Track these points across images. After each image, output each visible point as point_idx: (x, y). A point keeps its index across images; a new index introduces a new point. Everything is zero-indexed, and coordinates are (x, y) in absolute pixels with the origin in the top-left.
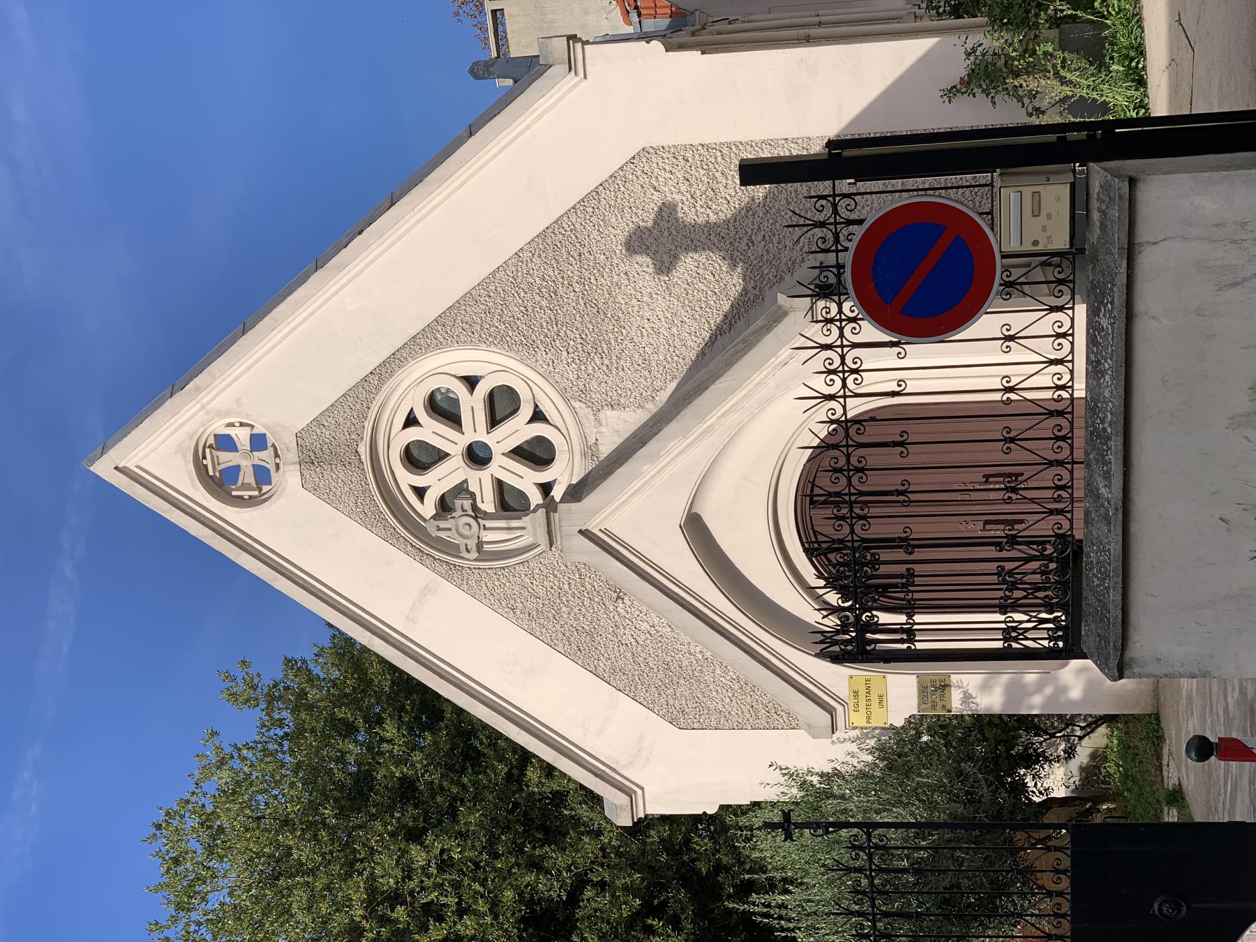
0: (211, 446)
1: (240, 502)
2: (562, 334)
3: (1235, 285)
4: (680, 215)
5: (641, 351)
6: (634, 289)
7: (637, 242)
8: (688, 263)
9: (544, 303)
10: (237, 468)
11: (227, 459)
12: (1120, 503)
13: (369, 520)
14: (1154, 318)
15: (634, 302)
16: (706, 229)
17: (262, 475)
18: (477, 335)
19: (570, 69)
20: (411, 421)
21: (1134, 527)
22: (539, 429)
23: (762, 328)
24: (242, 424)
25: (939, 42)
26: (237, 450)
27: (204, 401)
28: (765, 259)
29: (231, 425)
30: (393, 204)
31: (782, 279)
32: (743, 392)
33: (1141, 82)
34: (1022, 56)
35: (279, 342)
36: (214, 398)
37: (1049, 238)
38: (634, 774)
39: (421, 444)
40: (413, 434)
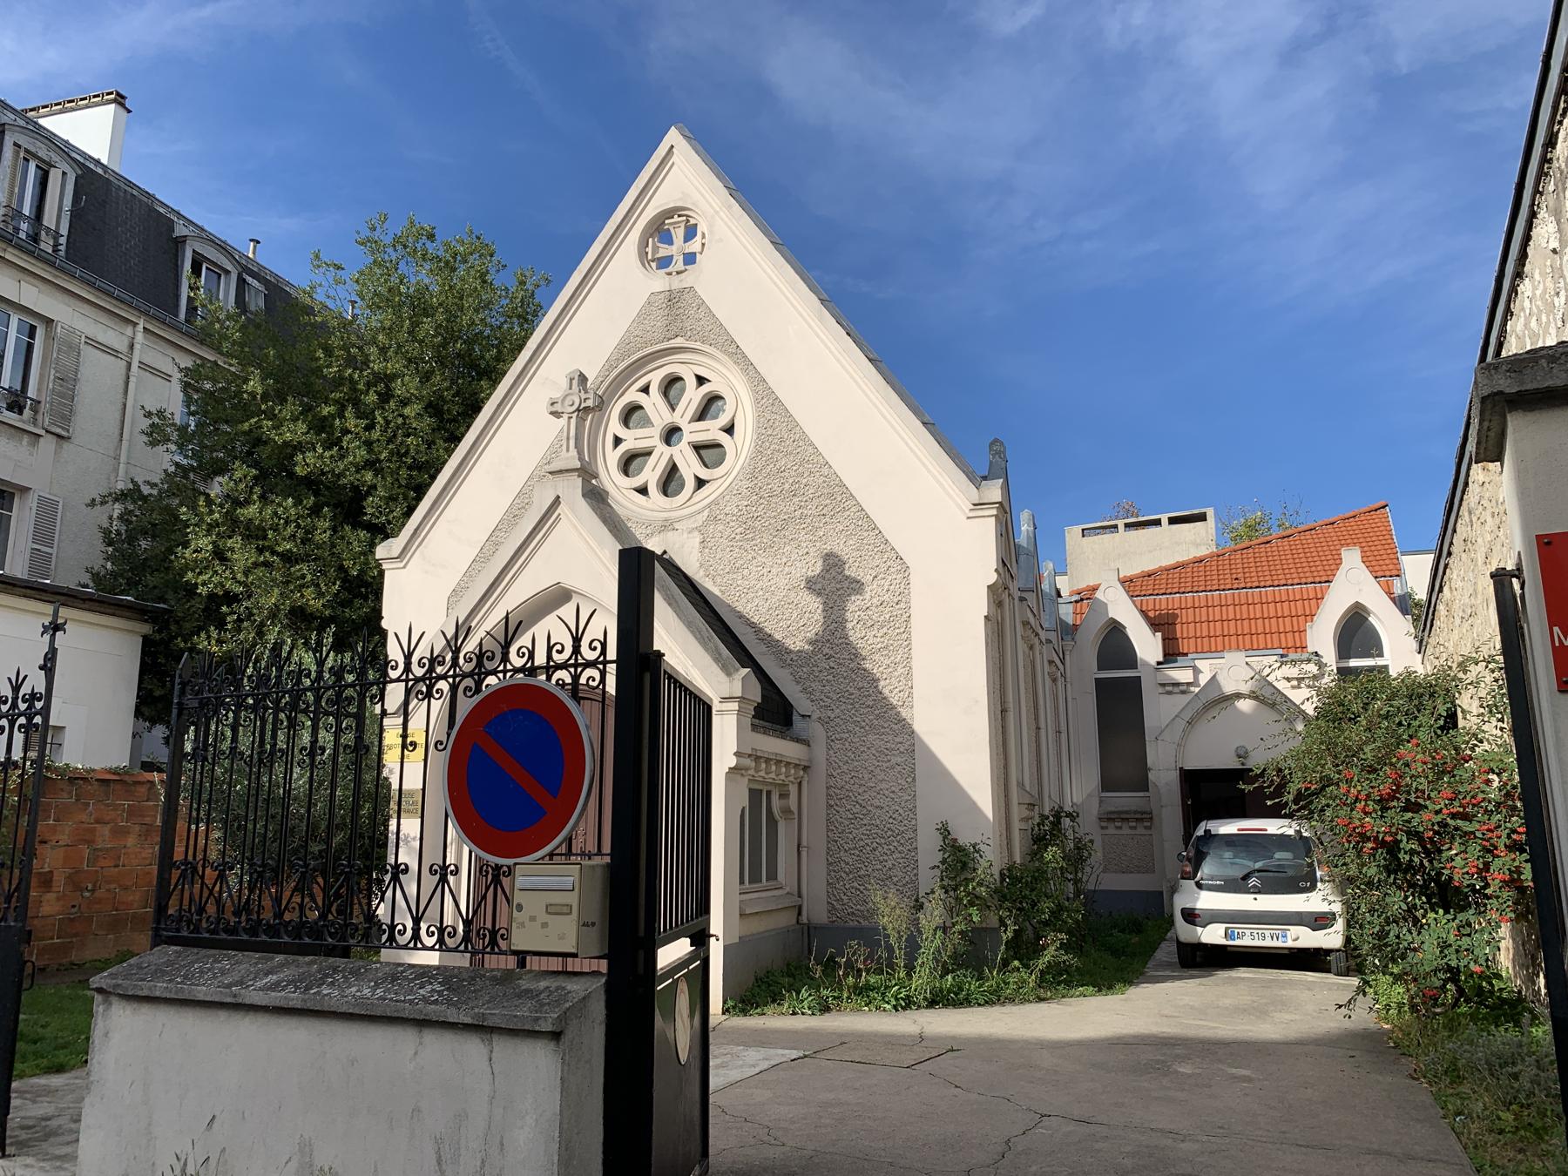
0: (688, 221)
1: (643, 244)
2: (761, 501)
3: (439, 1162)
4: (853, 598)
5: (746, 566)
6: (795, 560)
7: (833, 563)
8: (814, 604)
9: (787, 486)
10: (671, 243)
11: (678, 234)
12: (240, 1001)
13: (624, 346)
14: (416, 1053)
15: (784, 560)
16: (840, 619)
17: (664, 262)
18: (764, 431)
19: (974, 505)
20: (701, 380)
21: (223, 1015)
22: (690, 484)
23: (720, 655)
24: (703, 244)
25: (988, 820)
26: (685, 241)
27: (722, 213)
28: (815, 669)
29: (704, 236)
30: (870, 360)
31: (798, 683)
32: (665, 637)
33: (932, 1004)
34: (969, 894)
35: (765, 272)
36: (722, 220)
37: (522, 925)
38: (416, 561)
39: (683, 390)
40: (691, 382)
